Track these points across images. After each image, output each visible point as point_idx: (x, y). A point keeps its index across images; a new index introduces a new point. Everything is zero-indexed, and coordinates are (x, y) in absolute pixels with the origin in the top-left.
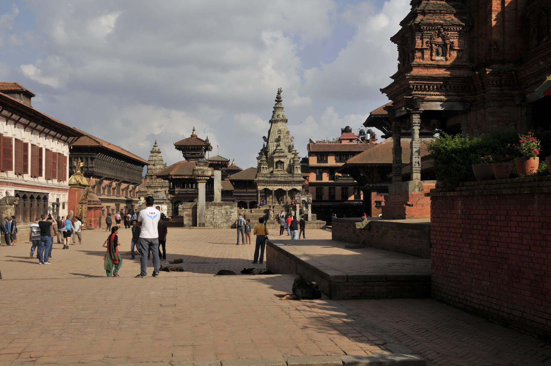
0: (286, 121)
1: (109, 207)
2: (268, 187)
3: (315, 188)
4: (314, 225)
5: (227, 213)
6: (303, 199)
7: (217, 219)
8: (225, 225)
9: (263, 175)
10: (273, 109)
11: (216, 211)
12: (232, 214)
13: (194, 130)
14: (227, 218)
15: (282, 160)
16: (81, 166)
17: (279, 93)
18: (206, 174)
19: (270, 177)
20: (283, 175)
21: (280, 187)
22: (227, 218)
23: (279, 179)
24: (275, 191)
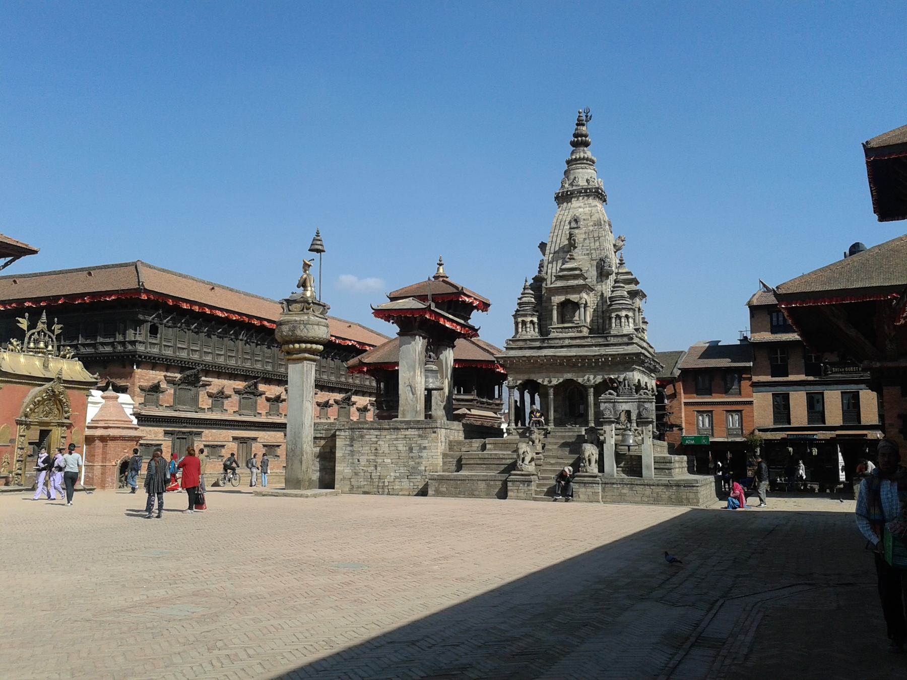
0: (598, 194)
1: (255, 439)
2: (533, 377)
3: (769, 397)
4: (659, 489)
5: (411, 449)
6: (625, 407)
7: (385, 466)
8: (406, 484)
9: (521, 344)
10: (566, 167)
11: (384, 446)
12: (424, 454)
13: (440, 265)
14: (412, 463)
15: (574, 297)
16: (57, 332)
17: (580, 124)
18: (302, 333)
19: (540, 348)
20: (578, 342)
21: (569, 376)
22: (412, 463)
23: (563, 352)
24: (556, 387)
